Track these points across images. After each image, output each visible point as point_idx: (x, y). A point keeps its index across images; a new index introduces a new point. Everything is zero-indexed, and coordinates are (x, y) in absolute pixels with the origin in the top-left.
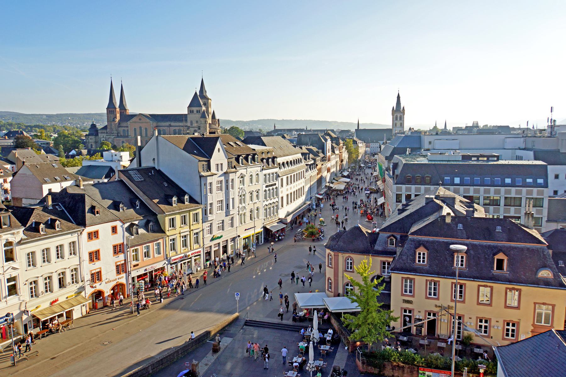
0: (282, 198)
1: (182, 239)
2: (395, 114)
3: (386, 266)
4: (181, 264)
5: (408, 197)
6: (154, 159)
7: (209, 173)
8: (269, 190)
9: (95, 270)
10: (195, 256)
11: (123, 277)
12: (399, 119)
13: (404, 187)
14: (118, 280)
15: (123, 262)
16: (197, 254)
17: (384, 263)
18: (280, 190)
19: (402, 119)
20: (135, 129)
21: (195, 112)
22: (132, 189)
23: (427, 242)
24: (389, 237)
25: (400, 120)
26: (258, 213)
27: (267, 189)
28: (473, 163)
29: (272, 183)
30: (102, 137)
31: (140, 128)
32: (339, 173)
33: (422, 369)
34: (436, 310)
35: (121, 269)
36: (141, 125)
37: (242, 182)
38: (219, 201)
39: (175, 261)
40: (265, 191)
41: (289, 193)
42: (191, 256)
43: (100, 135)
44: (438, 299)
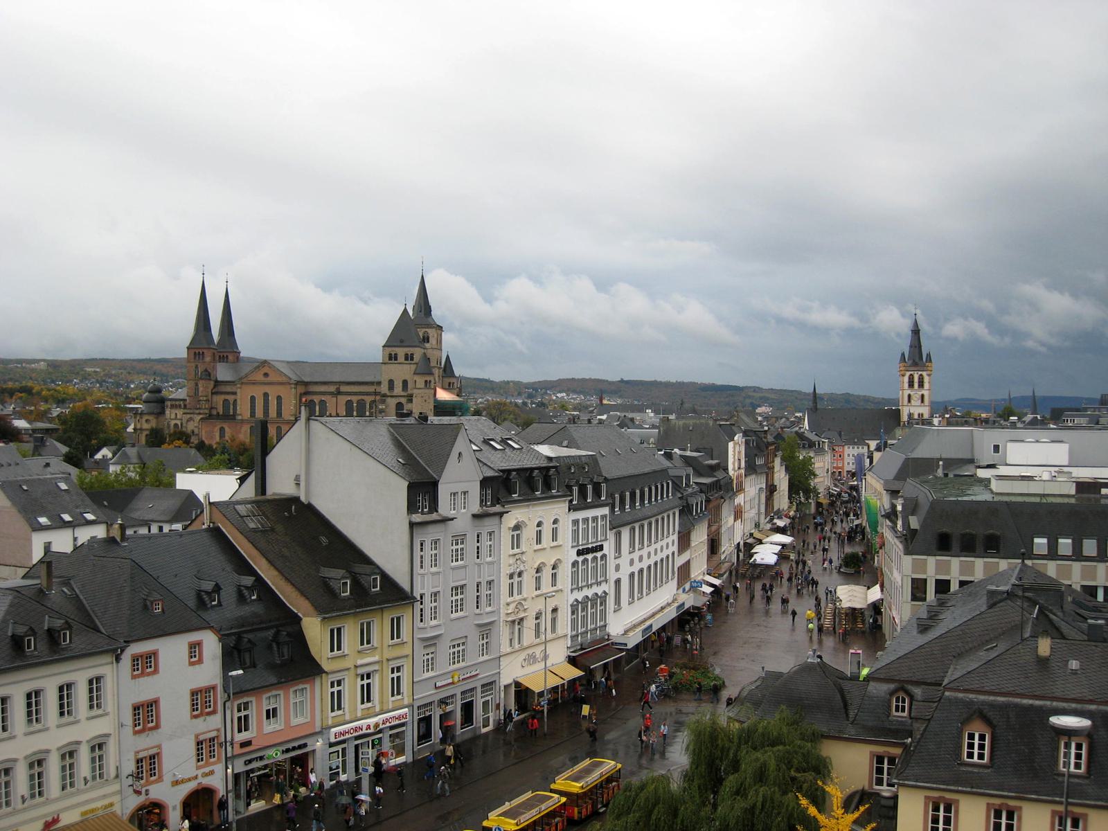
0: (618, 582)
1: (359, 683)
3: (886, 766)
4: (357, 747)
5: (943, 586)
6: (297, 478)
7: (434, 516)
8: (585, 561)
10: (392, 728)
11: (212, 773)
12: (916, 385)
13: (931, 561)
14: (200, 780)
15: (214, 734)
16: (397, 722)
17: (880, 760)
18: (611, 563)
20: (253, 399)
21: (401, 358)
22: (242, 552)
23: (992, 705)
24: (892, 693)
26: (554, 620)
27: (581, 559)
29: (594, 545)
30: (173, 416)
31: (266, 395)
32: (763, 520)
36: (267, 389)
37: (516, 542)
38: (457, 588)
39: (342, 738)
40: (575, 564)
41: (636, 569)
42: (381, 727)
43: (168, 412)
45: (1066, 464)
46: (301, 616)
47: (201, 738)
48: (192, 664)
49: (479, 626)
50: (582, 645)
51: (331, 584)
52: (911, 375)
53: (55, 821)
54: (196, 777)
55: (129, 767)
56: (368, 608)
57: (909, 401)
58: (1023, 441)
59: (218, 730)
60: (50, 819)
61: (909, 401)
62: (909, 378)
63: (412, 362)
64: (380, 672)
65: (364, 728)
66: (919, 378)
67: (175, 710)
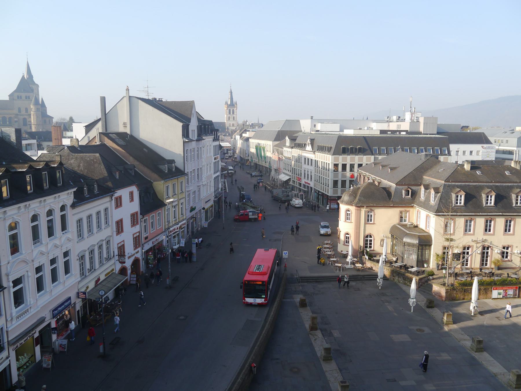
2: (229, 109)
9: (120, 243)
12: (231, 113)
13: (341, 157)
15: (138, 234)
19: (235, 113)
21: (23, 98)
22: (119, 155)
25: (233, 114)
28: (388, 136)
33: (495, 289)
34: (471, 244)
35: (137, 241)
44: (474, 234)
45: (339, 131)
46: (152, 181)
47: (135, 236)
48: (130, 202)
49: (198, 186)
50: (216, 196)
51: (160, 167)
52: (230, 109)
53: (99, 279)
54: (134, 254)
55: (116, 253)
56: (173, 178)
57: (229, 119)
58: (323, 123)
59: (139, 232)
60: (96, 279)
61: (229, 119)
62: (229, 111)
63: (29, 100)
64: (178, 205)
65: (176, 229)
66: (233, 111)
67: (127, 223)
